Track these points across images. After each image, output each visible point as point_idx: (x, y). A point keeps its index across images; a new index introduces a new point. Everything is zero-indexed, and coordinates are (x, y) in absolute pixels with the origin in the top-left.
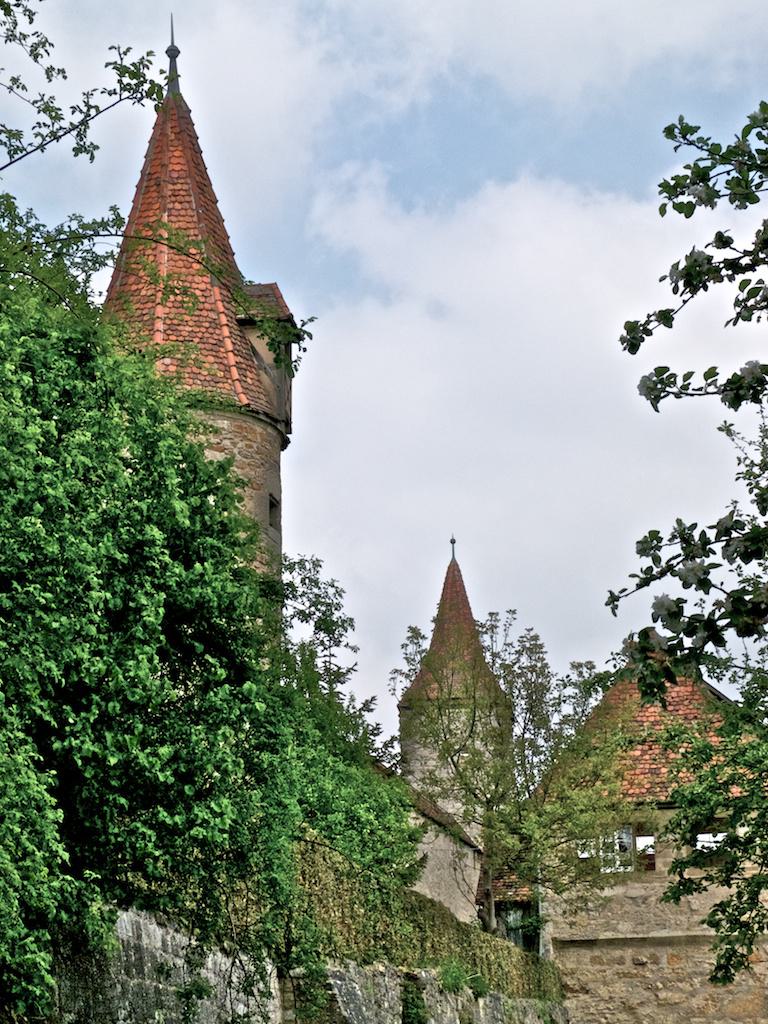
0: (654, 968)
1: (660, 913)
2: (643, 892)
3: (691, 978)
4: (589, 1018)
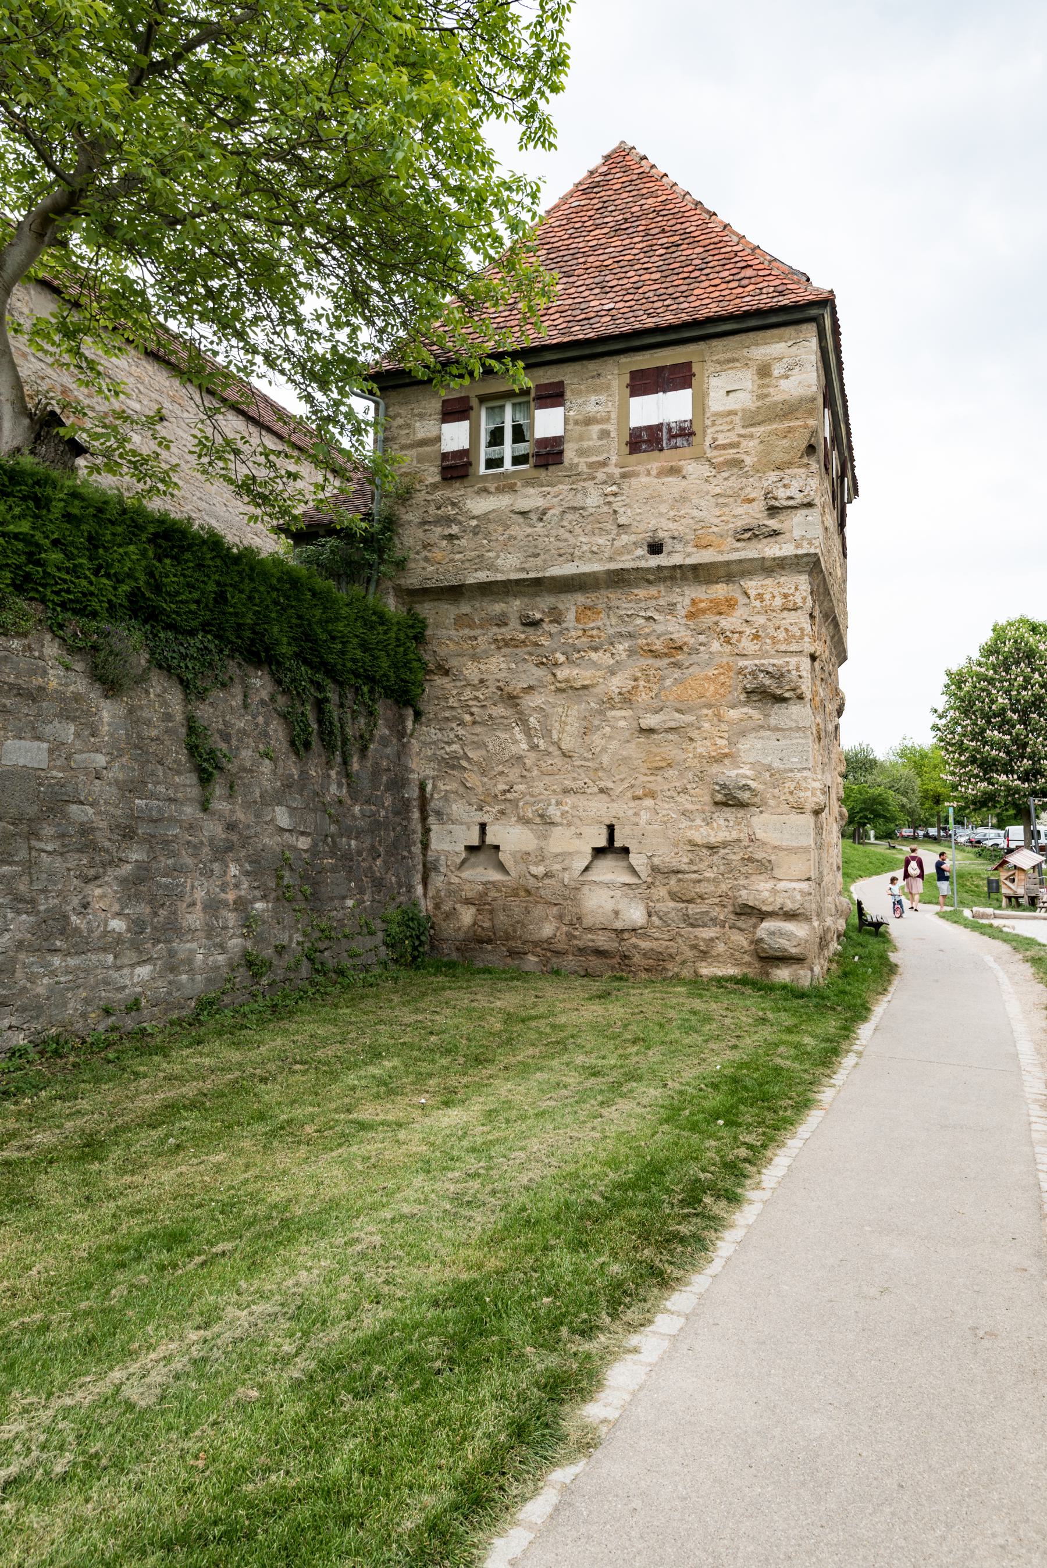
0: (554, 628)
1: (567, 535)
2: (541, 503)
3: (612, 644)
4: (447, 714)
